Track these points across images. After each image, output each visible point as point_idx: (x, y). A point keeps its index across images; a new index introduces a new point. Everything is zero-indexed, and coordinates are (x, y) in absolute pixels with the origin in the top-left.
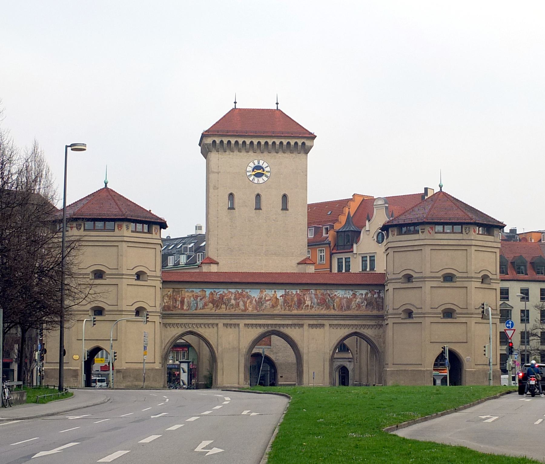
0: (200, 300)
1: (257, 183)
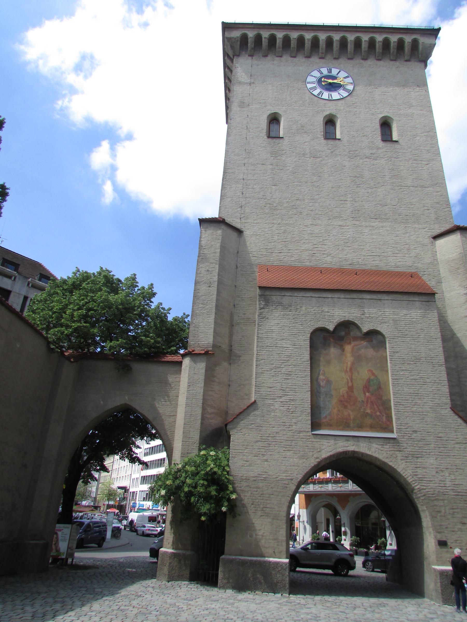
1: (327, 98)
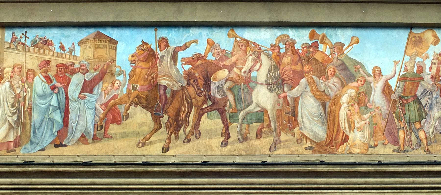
0: (83, 90)
